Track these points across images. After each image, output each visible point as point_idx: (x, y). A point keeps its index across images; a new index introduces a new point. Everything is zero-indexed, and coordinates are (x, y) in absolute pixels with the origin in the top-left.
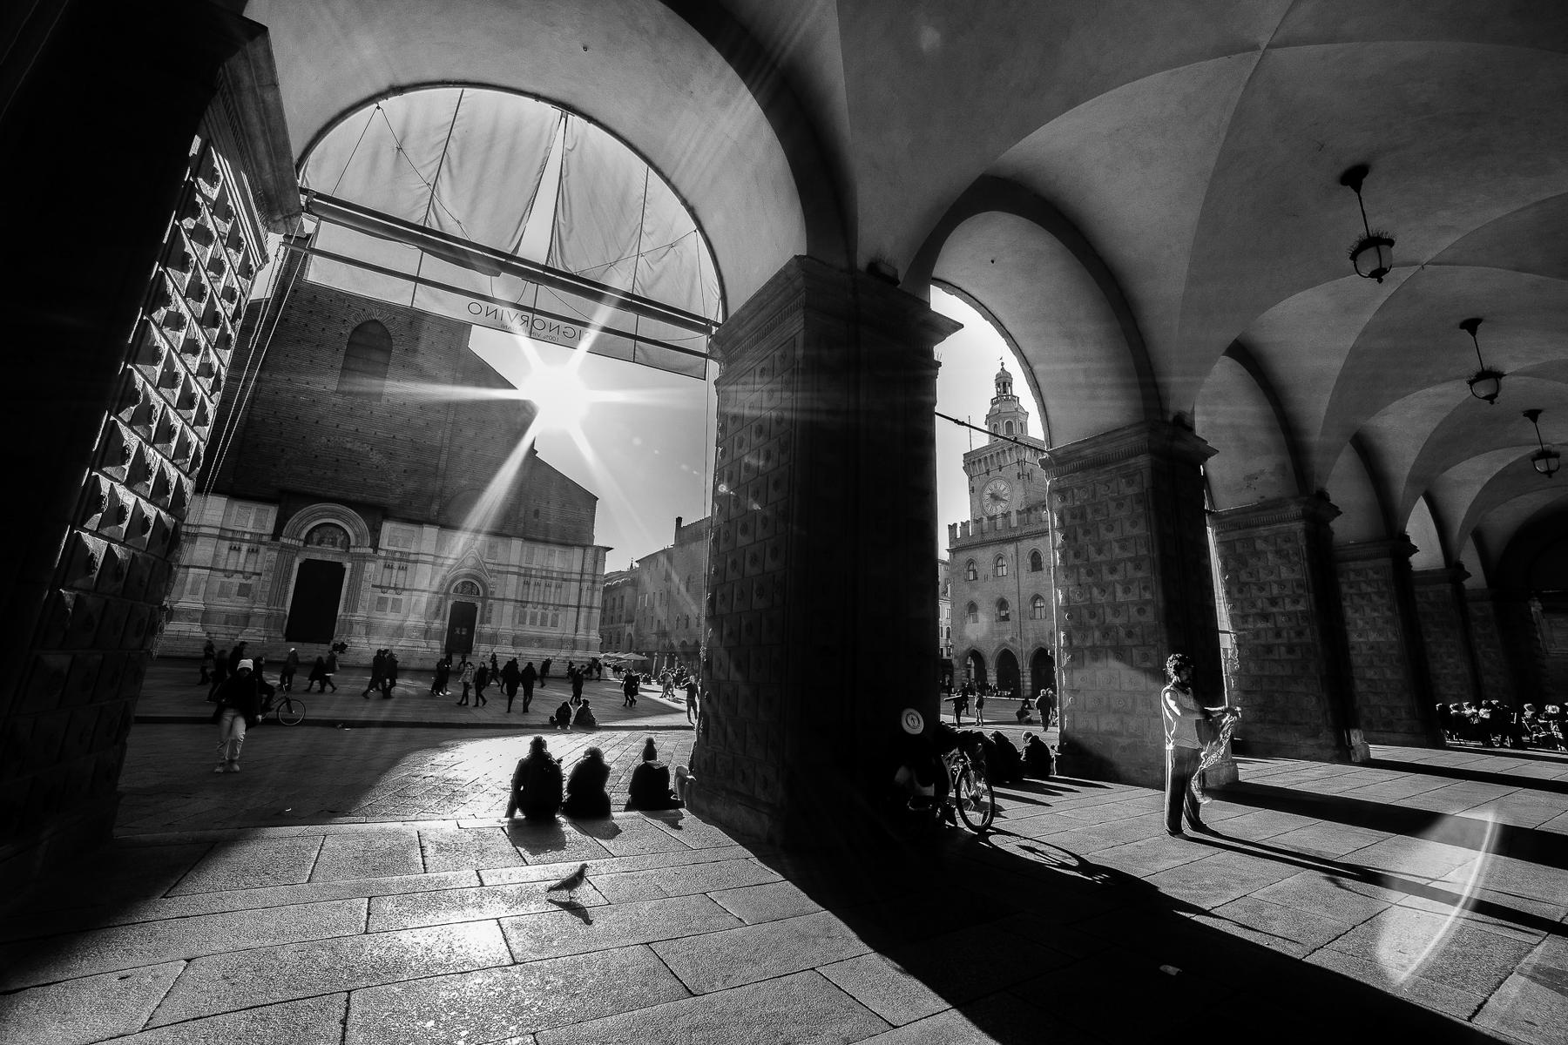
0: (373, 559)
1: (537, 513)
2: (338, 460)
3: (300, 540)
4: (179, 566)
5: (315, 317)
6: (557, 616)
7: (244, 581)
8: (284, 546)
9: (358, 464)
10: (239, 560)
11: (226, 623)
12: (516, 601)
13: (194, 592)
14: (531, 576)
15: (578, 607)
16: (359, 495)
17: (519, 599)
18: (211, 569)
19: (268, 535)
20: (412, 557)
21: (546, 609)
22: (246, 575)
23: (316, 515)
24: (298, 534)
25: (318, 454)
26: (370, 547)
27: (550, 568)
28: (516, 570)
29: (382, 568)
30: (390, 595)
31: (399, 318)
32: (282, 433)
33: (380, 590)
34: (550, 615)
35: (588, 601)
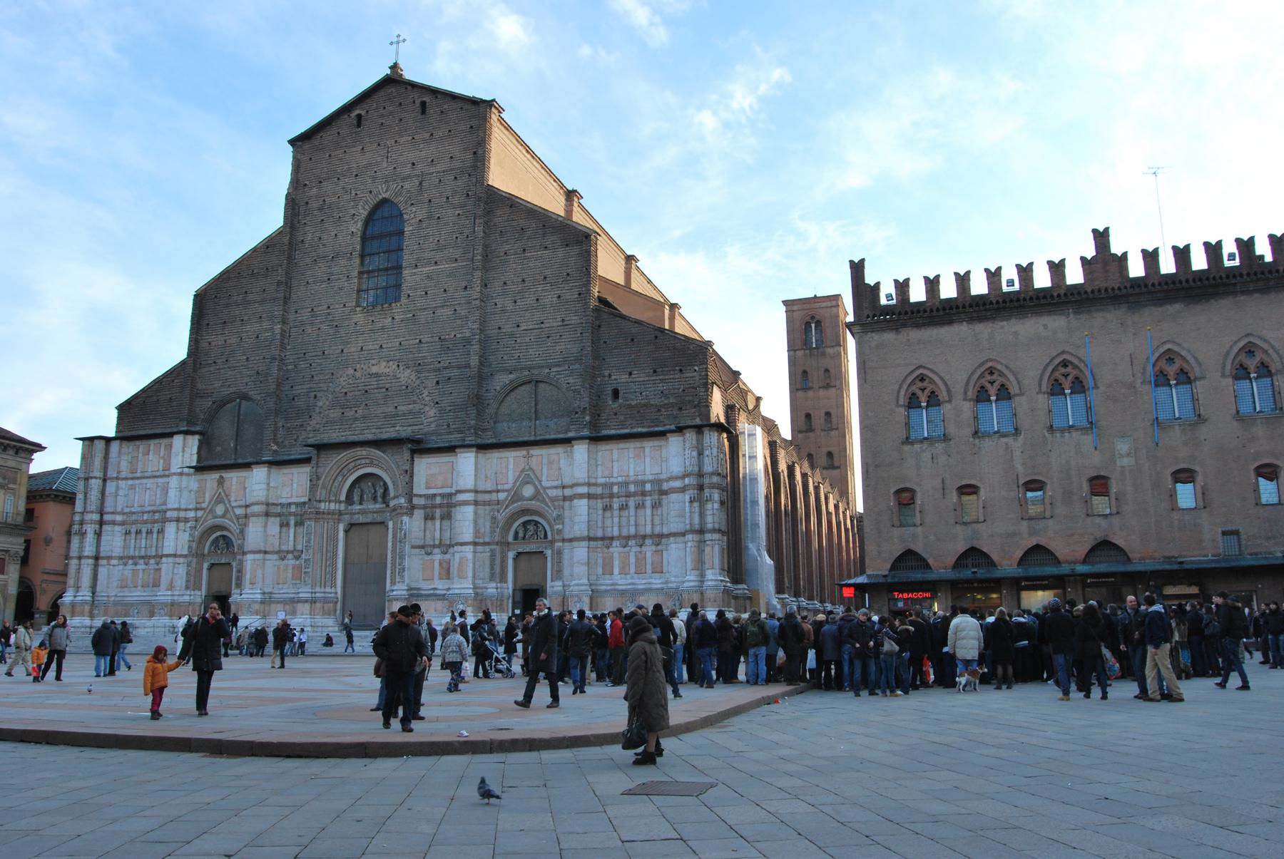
2: (366, 391)
3: (340, 502)
4: (244, 553)
9: (387, 389)
12: (590, 539)
14: (611, 496)
17: (600, 534)
18: (265, 552)
22: (296, 554)
24: (337, 494)
25: (346, 391)
28: (584, 490)
30: (437, 556)
31: (407, 185)
32: (313, 377)
33: (423, 552)
34: (649, 554)
35: (696, 520)
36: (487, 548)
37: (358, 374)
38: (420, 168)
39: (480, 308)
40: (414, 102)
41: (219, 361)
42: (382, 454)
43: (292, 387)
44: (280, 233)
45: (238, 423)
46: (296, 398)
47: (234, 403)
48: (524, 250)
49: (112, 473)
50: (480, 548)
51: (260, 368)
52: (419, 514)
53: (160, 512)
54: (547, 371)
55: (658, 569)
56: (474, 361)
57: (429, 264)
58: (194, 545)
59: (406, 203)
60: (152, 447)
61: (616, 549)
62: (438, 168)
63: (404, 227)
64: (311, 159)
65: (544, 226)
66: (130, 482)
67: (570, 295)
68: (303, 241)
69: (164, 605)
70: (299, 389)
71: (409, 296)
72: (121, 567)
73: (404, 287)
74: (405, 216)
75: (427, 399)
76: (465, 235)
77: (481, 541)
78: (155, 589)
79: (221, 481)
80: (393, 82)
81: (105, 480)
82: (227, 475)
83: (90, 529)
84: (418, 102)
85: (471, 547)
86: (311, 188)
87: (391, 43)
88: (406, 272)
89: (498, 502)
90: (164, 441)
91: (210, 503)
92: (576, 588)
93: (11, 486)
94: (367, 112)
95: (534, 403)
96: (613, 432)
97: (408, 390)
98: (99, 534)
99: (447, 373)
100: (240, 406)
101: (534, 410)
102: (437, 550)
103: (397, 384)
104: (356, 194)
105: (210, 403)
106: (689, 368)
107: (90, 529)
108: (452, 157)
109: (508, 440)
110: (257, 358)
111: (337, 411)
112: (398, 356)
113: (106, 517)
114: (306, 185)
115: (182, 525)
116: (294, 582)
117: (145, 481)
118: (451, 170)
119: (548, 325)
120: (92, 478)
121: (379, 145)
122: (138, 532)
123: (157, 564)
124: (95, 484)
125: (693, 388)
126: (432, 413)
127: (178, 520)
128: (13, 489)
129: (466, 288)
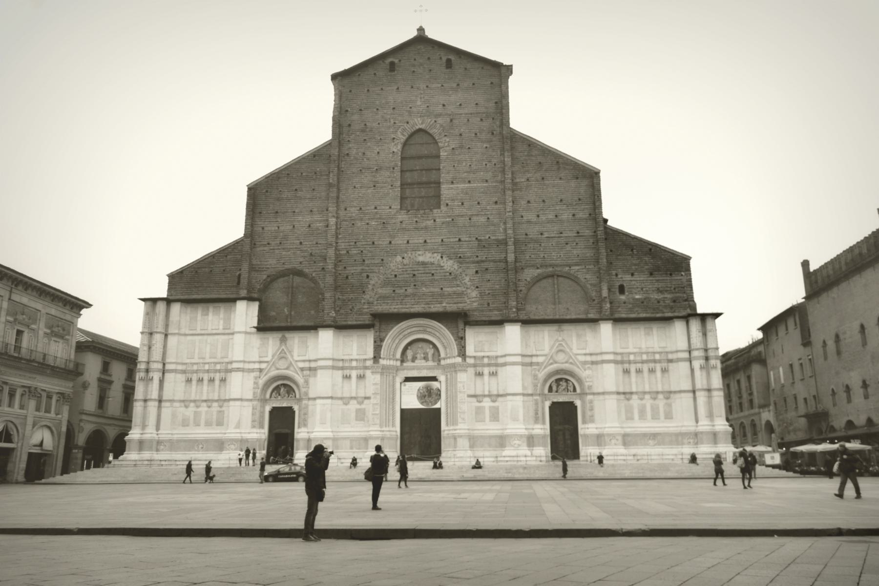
0: (464, 368)
1: (622, 290)
2: (414, 275)
3: (397, 360)
4: (309, 399)
5: (369, 144)
6: (669, 405)
7: (358, 407)
8: (384, 368)
9: (433, 274)
10: (352, 388)
11: (351, 448)
12: (618, 393)
13: (323, 423)
14: (630, 362)
15: (694, 392)
16: (439, 305)
17: (621, 390)
18: (332, 398)
19: (369, 359)
20: (501, 361)
21: (655, 399)
22: (360, 400)
23: (406, 333)
24: (394, 355)
25: (396, 273)
26: (459, 356)
27: (651, 350)
28: (611, 357)
29: (473, 375)
30: (487, 403)
31: (440, 121)
32: (364, 261)
33: (474, 400)
35: (705, 382)
36: (531, 398)
37: (405, 261)
38: (451, 109)
39: (513, 218)
40: (441, 58)
41: (273, 243)
42: (439, 324)
43: (345, 268)
44: (328, 146)
45: (292, 293)
46: (349, 277)
47: (286, 278)
48: (543, 179)
49: (170, 331)
50: (526, 398)
51: (314, 252)
52: (471, 371)
53: (223, 363)
54: (567, 268)
55: (669, 416)
56: (511, 257)
57: (464, 182)
58: (259, 391)
59: (440, 134)
60: (211, 309)
61: (635, 401)
62: (466, 111)
63: (440, 152)
64: (350, 91)
65: (558, 162)
66: (189, 338)
67: (582, 214)
68: (348, 154)
69: (233, 441)
70: (351, 270)
71: (447, 205)
72: (183, 409)
73: (443, 198)
74: (440, 144)
75: (469, 283)
76: (493, 163)
77: (525, 392)
78: (219, 427)
79: (283, 340)
80: (421, 40)
81: (166, 335)
82: (288, 335)
83: (156, 376)
84: (444, 59)
85: (522, 397)
86: (353, 114)
87: (416, 11)
88: (443, 186)
89: (538, 364)
90: (222, 307)
91: (273, 356)
92: (610, 429)
93: (67, 337)
94: (400, 61)
95: (556, 291)
96: (624, 316)
97: (452, 277)
98: (161, 382)
99: (485, 265)
100: (293, 279)
101: (556, 297)
102: (487, 399)
103: (442, 271)
104: (395, 123)
105: (265, 277)
106: (676, 273)
107: (156, 376)
108: (477, 104)
109: (537, 318)
110: (310, 243)
111: (389, 288)
112: (441, 249)
113: (168, 367)
114: (347, 111)
115: (246, 374)
116: (358, 422)
117: (205, 337)
118: (477, 113)
119: (566, 235)
120: (157, 332)
121: (412, 87)
122: (200, 380)
123: (221, 407)
124: (158, 338)
125: (682, 287)
126: (474, 294)
127: (242, 370)
128: (67, 340)
129: (496, 202)
